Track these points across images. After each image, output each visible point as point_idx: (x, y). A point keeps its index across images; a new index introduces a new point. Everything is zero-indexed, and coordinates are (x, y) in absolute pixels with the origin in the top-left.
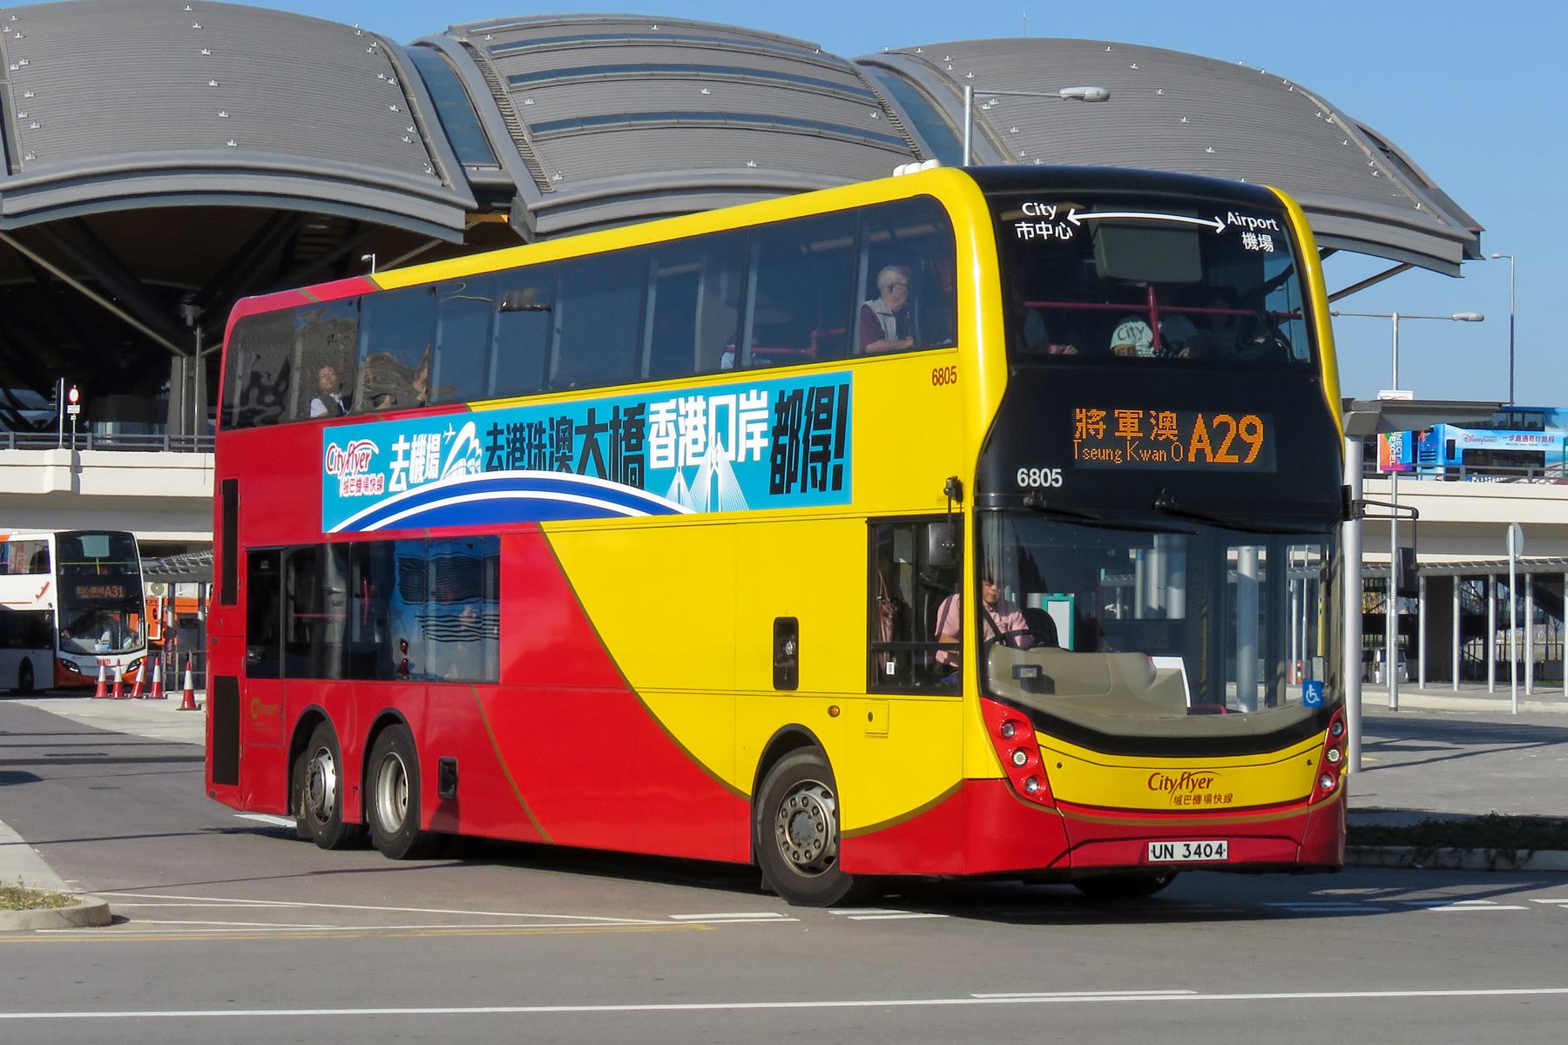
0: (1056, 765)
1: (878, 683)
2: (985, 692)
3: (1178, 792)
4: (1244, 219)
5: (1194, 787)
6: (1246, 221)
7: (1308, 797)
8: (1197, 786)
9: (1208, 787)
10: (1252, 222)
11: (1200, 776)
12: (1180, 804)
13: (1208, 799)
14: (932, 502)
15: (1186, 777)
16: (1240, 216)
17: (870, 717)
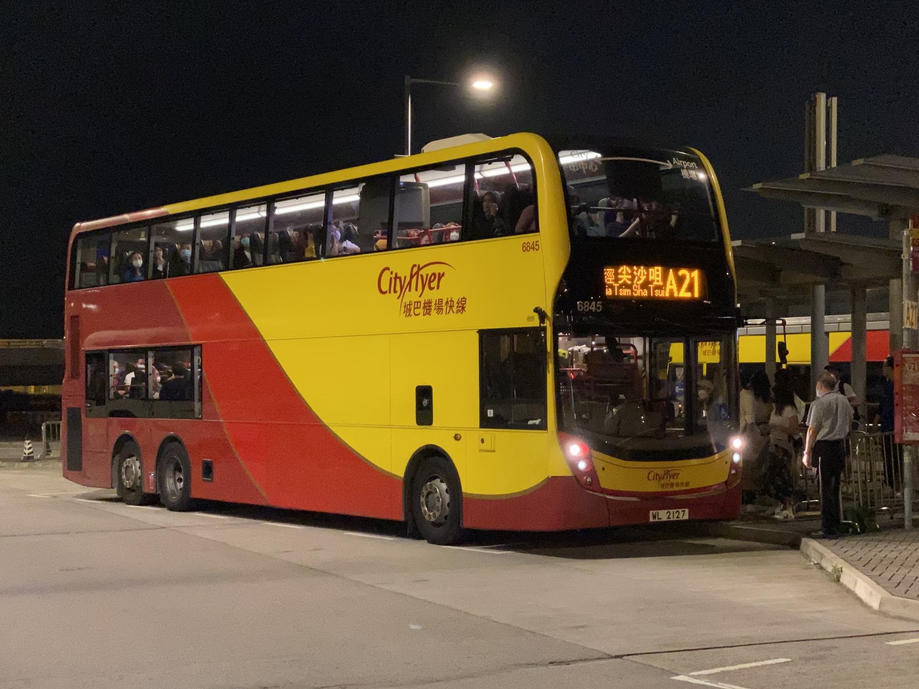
0: (601, 469)
1: (485, 422)
2: (562, 428)
3: (662, 482)
4: (681, 161)
5: (670, 478)
6: (682, 163)
7: (726, 482)
8: (672, 478)
9: (677, 478)
10: (685, 164)
11: (673, 472)
12: (663, 488)
13: (677, 485)
14: (524, 319)
15: (667, 472)
16: (679, 160)
17: (483, 441)
